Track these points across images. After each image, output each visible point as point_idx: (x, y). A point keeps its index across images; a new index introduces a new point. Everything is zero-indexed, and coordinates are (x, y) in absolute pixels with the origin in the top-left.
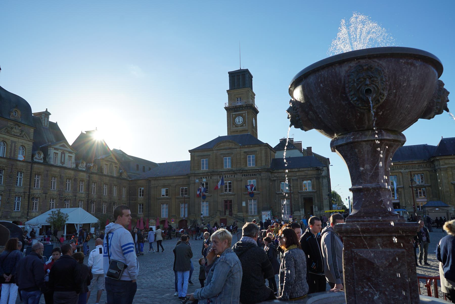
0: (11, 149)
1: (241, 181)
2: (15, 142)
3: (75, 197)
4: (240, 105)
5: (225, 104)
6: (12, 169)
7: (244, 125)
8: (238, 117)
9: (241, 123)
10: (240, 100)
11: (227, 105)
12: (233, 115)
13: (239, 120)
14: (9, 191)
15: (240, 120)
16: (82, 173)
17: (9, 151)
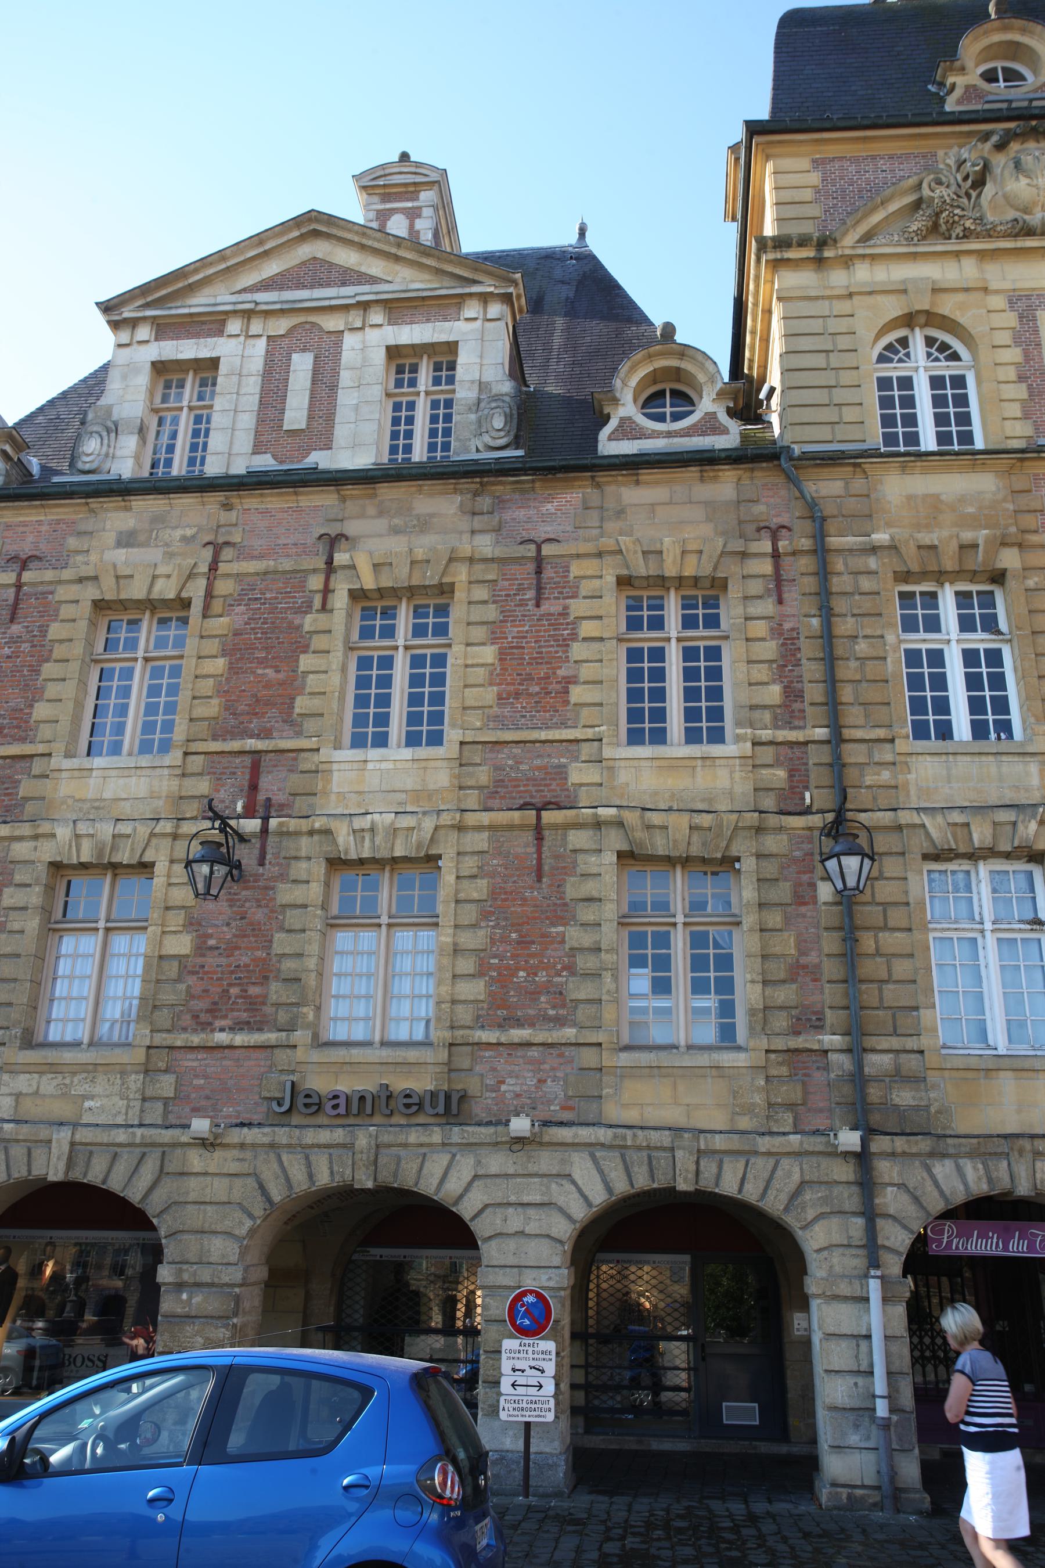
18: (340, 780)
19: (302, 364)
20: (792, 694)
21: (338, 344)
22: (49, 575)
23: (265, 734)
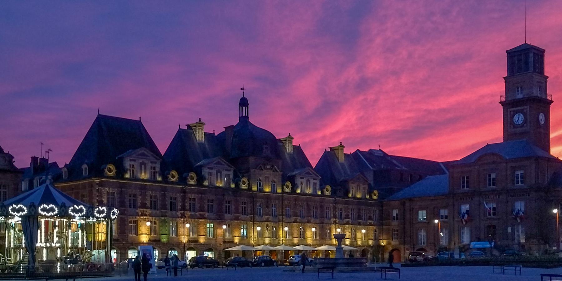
1: (507, 202)
3: (322, 224)
4: (520, 99)
5: (501, 96)
7: (525, 125)
8: (517, 114)
9: (522, 122)
10: (521, 91)
11: (503, 99)
12: (510, 112)
13: (519, 119)
15: (520, 119)
20: (251, 212)
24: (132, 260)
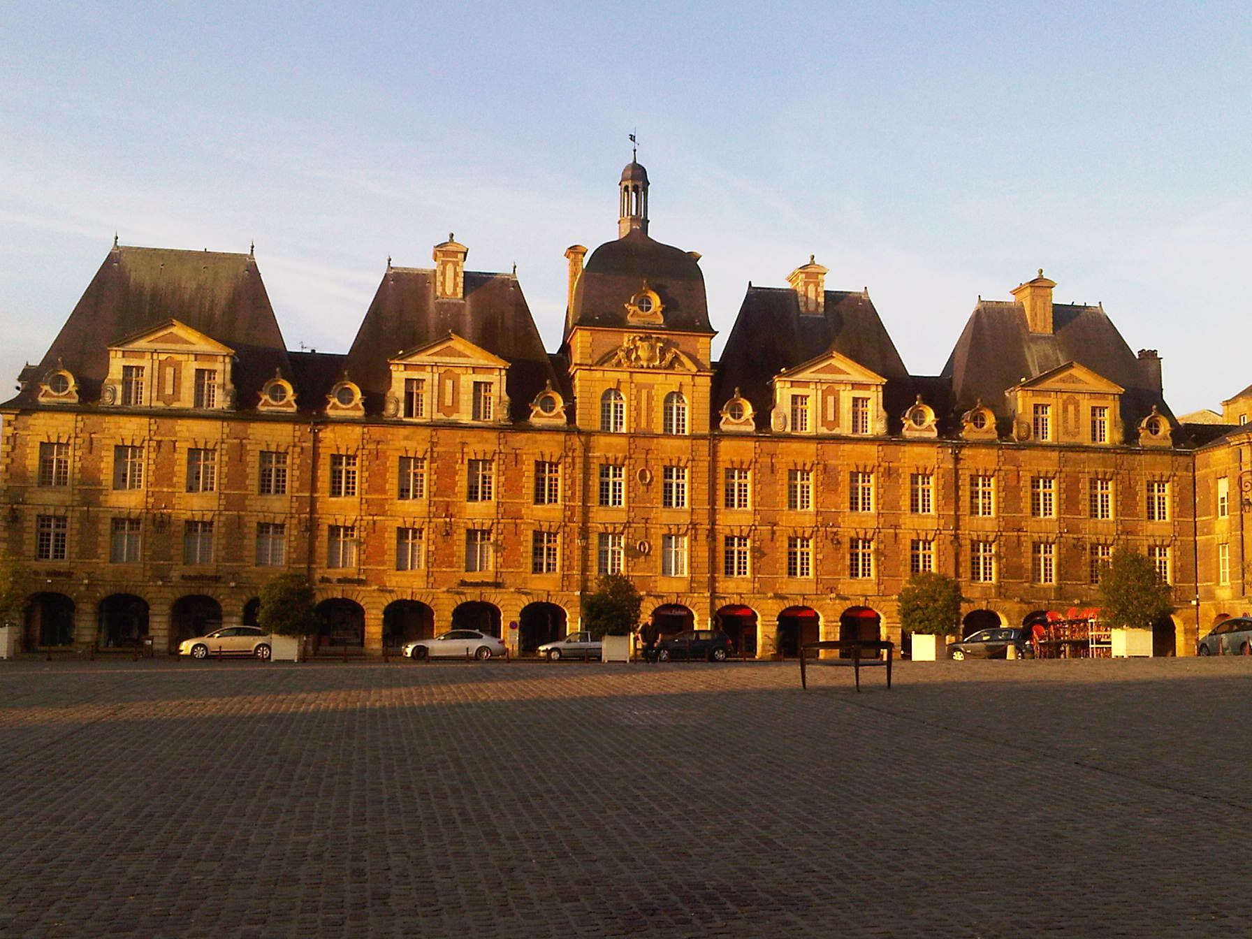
0: (638, 409)
2: (651, 387)
3: (892, 531)
6: (647, 462)
14: (644, 521)
16: (917, 449)
17: (634, 414)
18: (468, 510)
19: (449, 383)
21: (459, 378)
22: (385, 447)
23: (448, 497)
24: (149, 639)
